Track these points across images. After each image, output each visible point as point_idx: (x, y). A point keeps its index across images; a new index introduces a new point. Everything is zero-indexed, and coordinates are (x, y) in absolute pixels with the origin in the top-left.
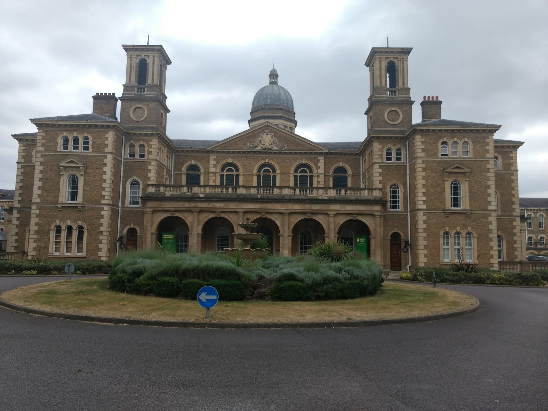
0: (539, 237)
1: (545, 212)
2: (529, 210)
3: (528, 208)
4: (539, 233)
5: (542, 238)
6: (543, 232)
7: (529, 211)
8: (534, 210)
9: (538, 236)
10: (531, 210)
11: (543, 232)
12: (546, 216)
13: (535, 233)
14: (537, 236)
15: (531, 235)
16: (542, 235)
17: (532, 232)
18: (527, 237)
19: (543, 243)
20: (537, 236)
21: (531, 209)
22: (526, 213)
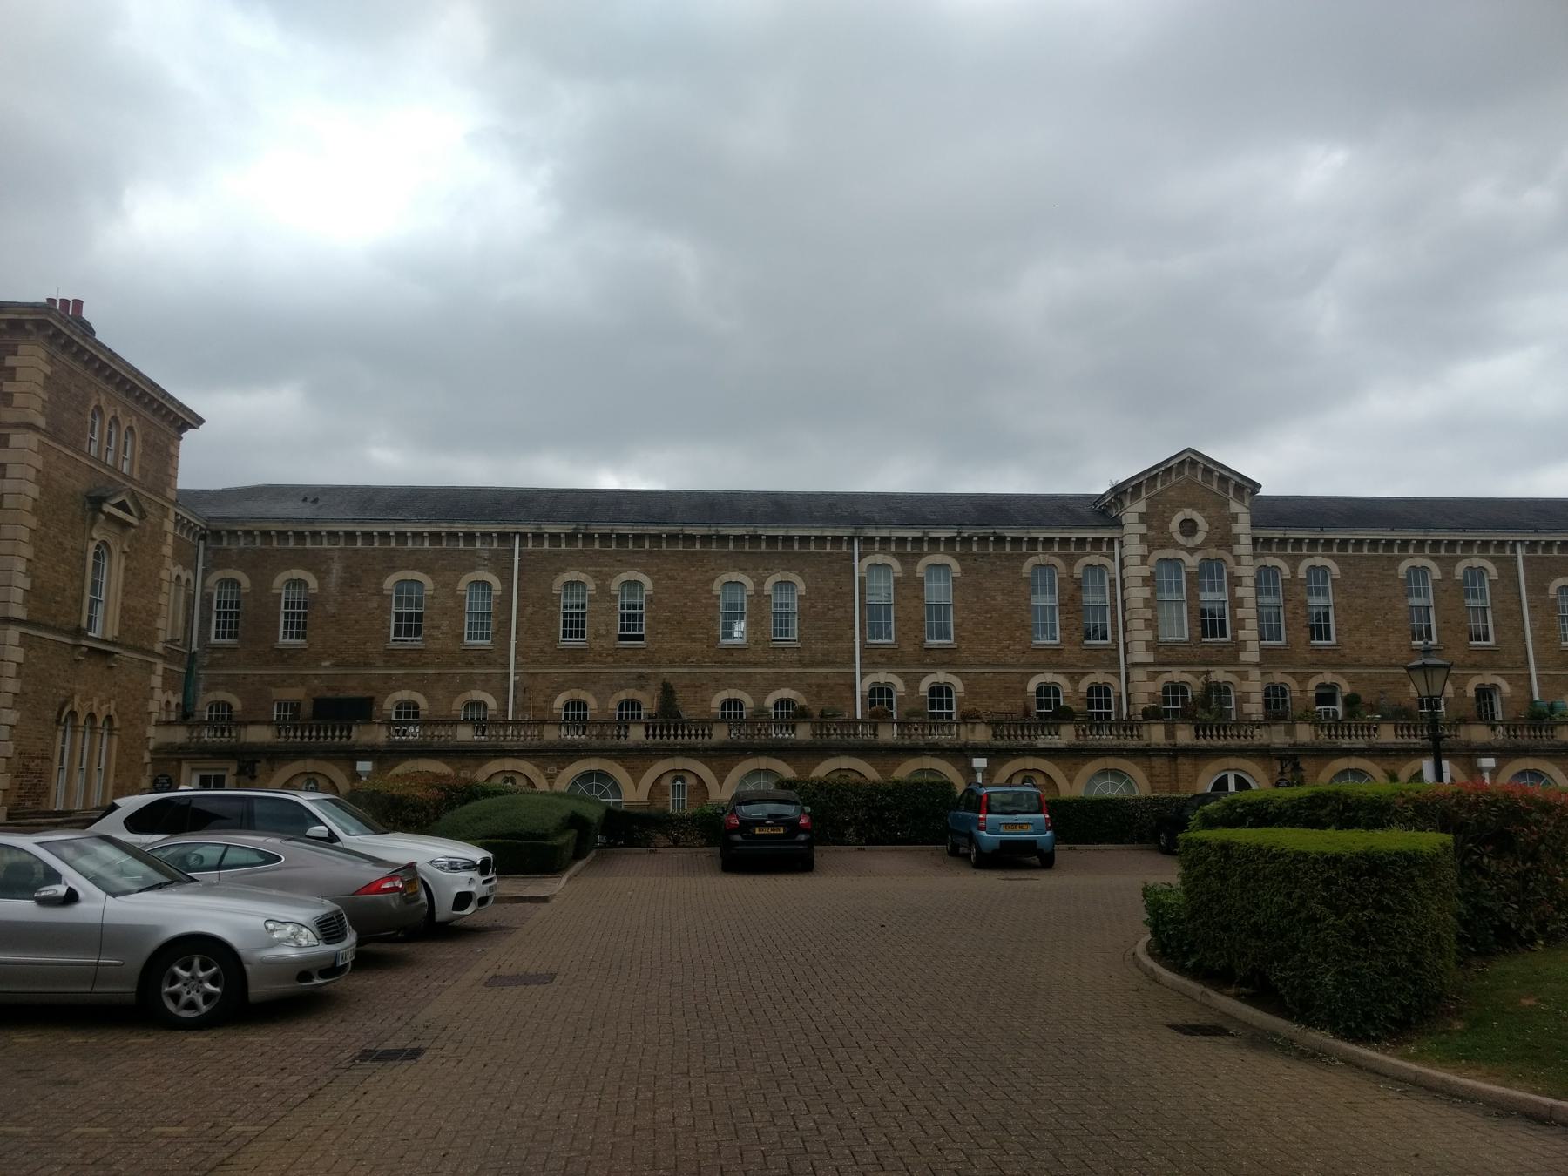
0: (924, 687)
1: (958, 549)
2: (872, 539)
3: (870, 532)
4: (925, 666)
5: (941, 693)
6: (946, 658)
7: (877, 546)
8: (902, 541)
9: (919, 679)
10: (885, 541)
11: (946, 658)
12: (965, 571)
13: (903, 665)
14: (912, 682)
15: (882, 677)
16: (941, 677)
17: (889, 658)
18: (862, 687)
19: (949, 716)
20: (912, 682)
21: (885, 533)
22: (861, 556)
